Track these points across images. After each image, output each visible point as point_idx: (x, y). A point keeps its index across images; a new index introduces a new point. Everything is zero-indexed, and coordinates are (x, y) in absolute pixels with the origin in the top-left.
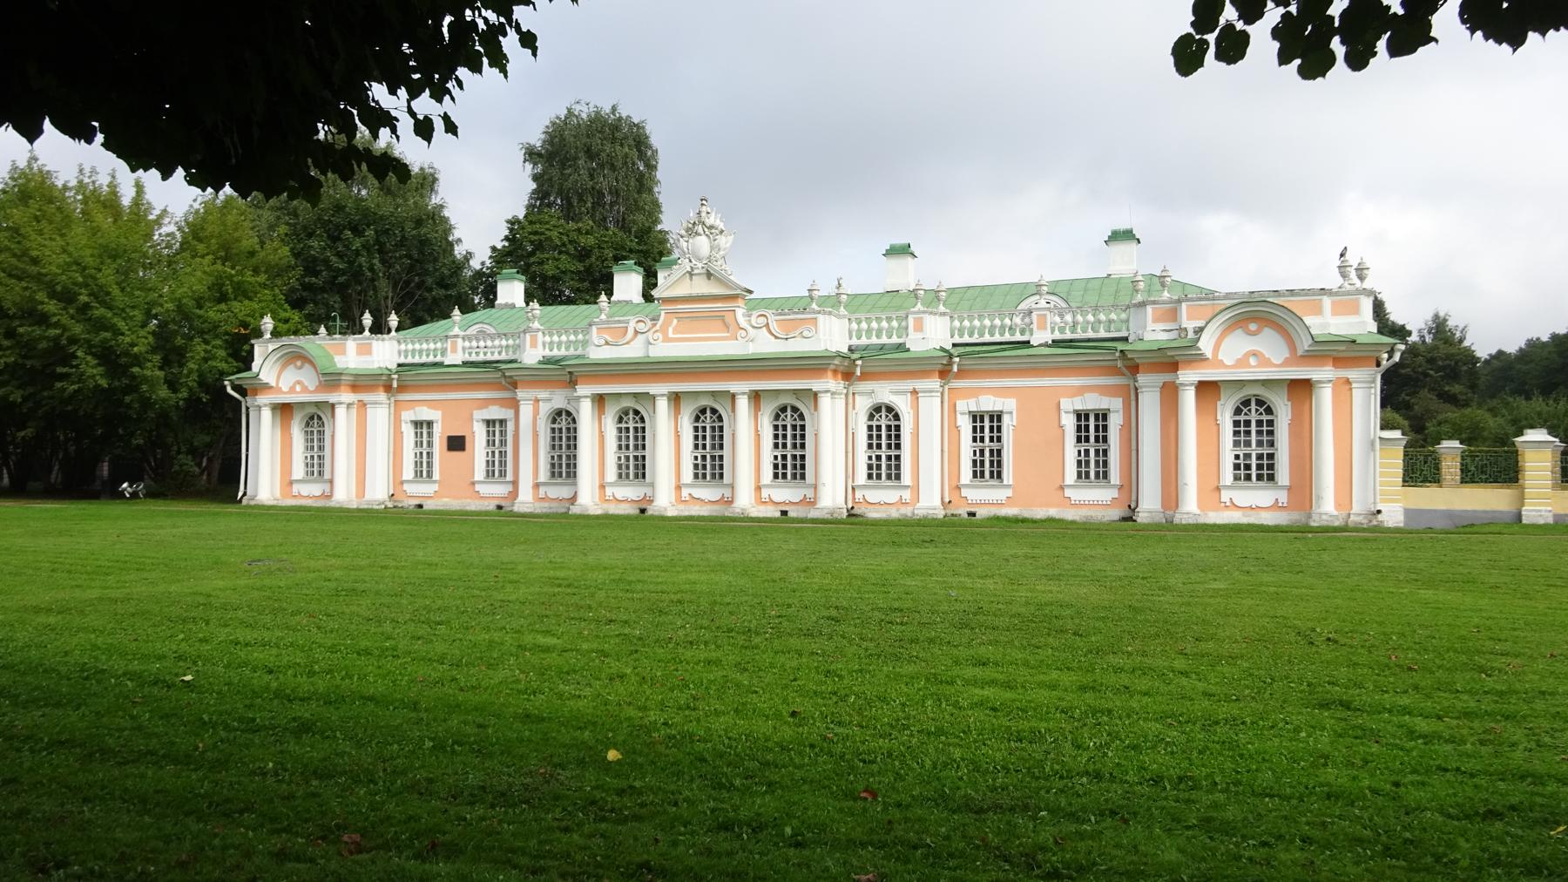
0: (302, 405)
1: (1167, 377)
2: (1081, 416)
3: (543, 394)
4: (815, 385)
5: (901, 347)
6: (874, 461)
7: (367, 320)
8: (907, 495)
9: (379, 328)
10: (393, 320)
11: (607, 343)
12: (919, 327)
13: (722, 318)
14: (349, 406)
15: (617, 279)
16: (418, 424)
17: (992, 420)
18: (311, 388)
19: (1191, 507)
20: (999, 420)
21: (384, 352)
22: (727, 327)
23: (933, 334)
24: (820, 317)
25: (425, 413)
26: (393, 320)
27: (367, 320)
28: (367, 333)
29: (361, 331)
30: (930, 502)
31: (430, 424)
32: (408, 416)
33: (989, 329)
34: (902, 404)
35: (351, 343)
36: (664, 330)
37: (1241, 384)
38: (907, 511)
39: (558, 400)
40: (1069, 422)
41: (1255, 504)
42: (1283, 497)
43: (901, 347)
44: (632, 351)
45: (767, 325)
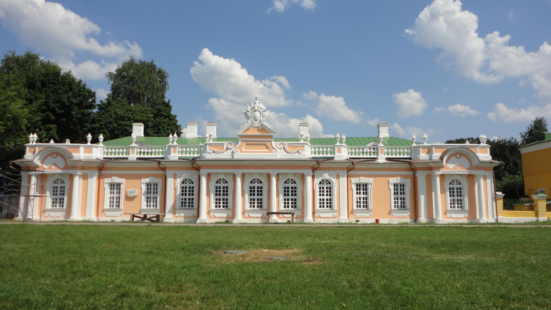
0: (53, 175)
1: (428, 172)
2: (395, 185)
3: (178, 172)
4: (304, 171)
5: (333, 158)
6: (184, 201)
7: (89, 136)
8: (335, 214)
9: (95, 141)
10: (101, 137)
11: (214, 152)
12: (339, 151)
13: (266, 145)
14: (80, 175)
15: (134, 127)
16: (112, 185)
17: (363, 186)
18: (62, 167)
19: (442, 219)
20: (366, 186)
21: (98, 152)
22: (267, 148)
23: (343, 154)
24: (306, 146)
25: (116, 180)
26: (101, 137)
27: (89, 136)
28: (89, 144)
29: (86, 142)
30: (344, 218)
31: (119, 185)
32: (355, 180)
33: (365, 153)
34: (334, 180)
35: (82, 147)
36: (240, 148)
37: (452, 175)
38: (336, 220)
39: (186, 175)
40: (392, 187)
41: (460, 218)
42: (467, 215)
43: (333, 158)
44: (226, 155)
45: (284, 148)
